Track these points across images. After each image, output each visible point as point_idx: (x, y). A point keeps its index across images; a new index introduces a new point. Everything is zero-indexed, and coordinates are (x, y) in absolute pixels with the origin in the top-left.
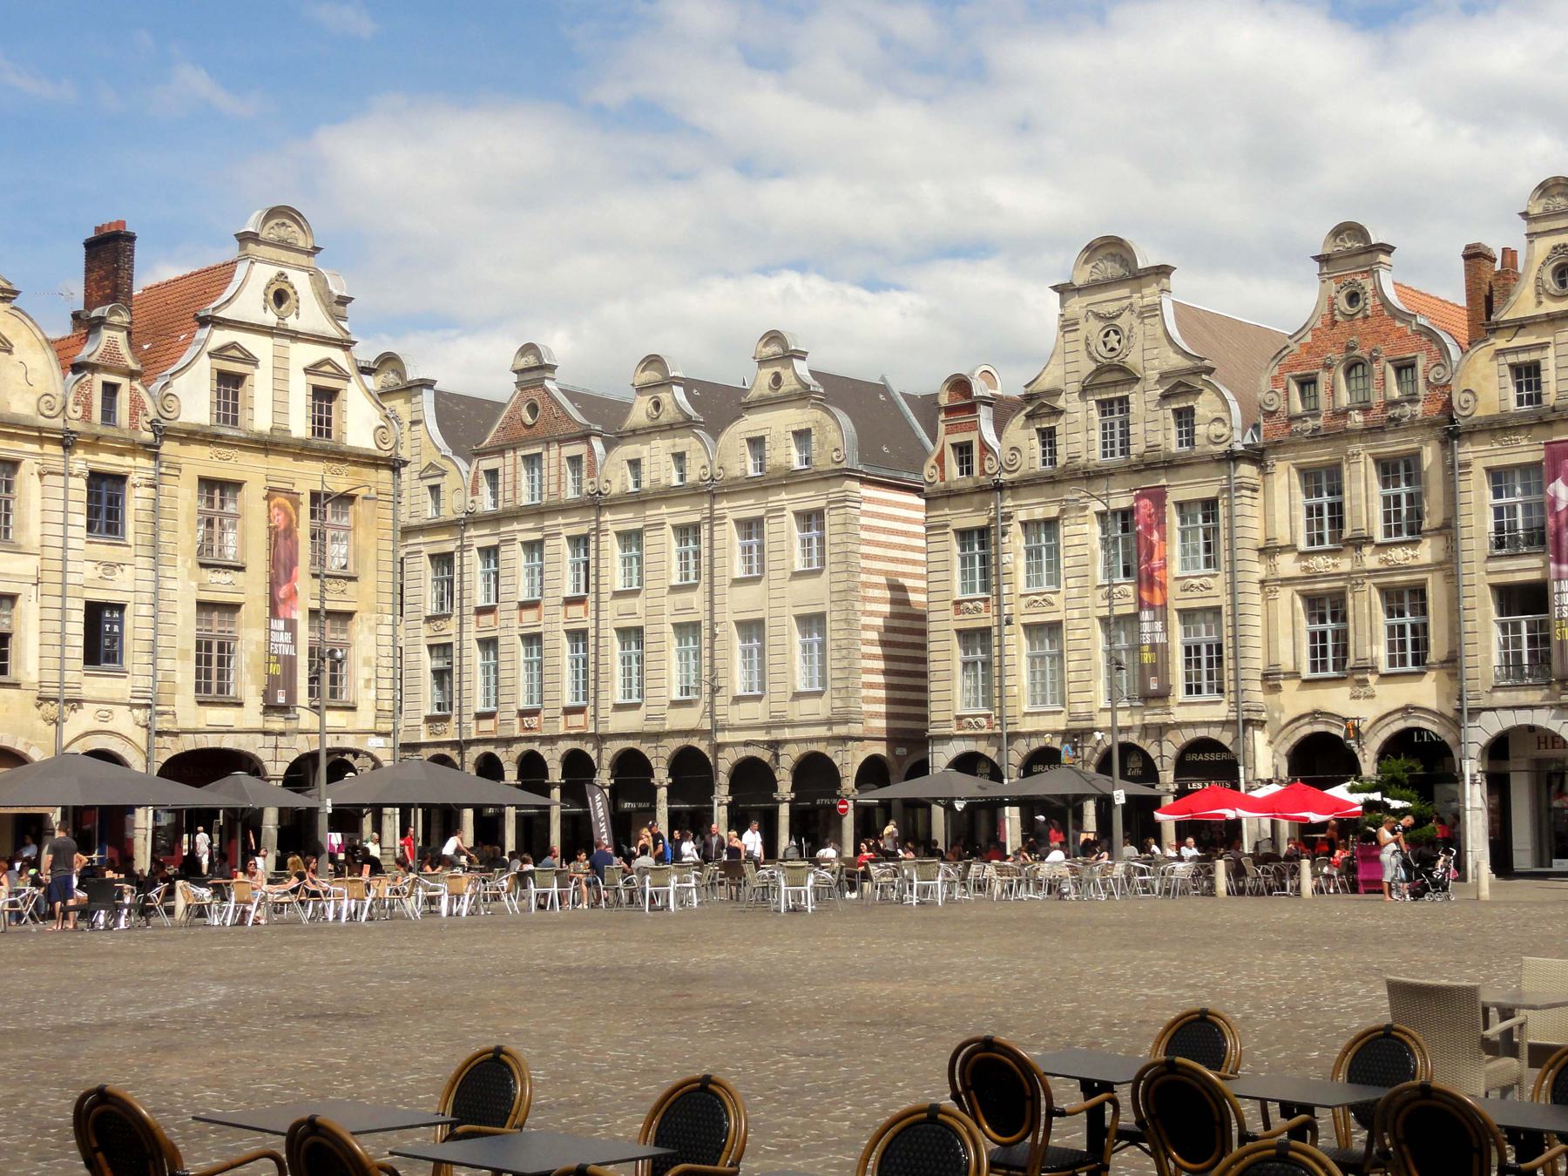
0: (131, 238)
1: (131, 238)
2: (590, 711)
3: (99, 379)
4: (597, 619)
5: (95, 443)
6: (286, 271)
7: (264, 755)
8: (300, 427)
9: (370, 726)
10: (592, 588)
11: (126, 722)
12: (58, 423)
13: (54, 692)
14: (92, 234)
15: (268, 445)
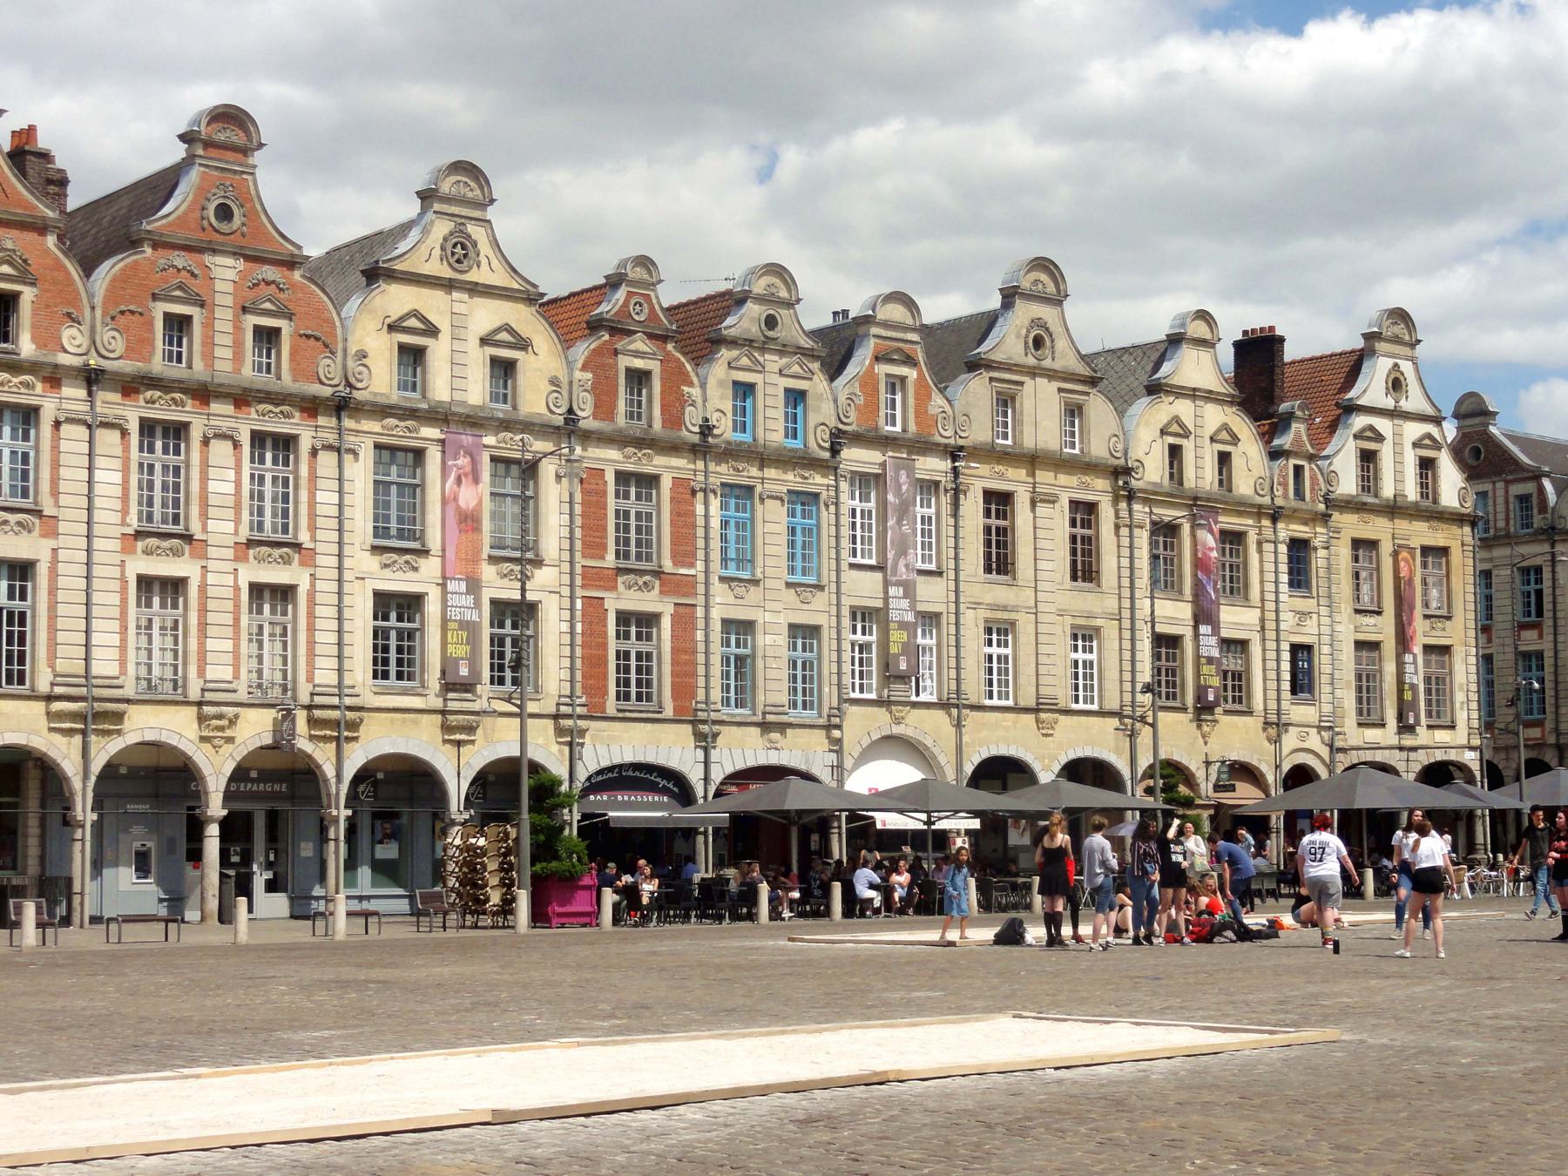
0: (1281, 340)
1: (1281, 340)
2: (1549, 725)
3: (1293, 461)
4: (1555, 642)
5: (1294, 516)
6: (1400, 362)
7: (1401, 767)
8: (1412, 493)
9: (1465, 742)
10: (1547, 614)
11: (1315, 741)
12: (1267, 500)
13: (1273, 718)
14: (1240, 337)
15: (1394, 509)
